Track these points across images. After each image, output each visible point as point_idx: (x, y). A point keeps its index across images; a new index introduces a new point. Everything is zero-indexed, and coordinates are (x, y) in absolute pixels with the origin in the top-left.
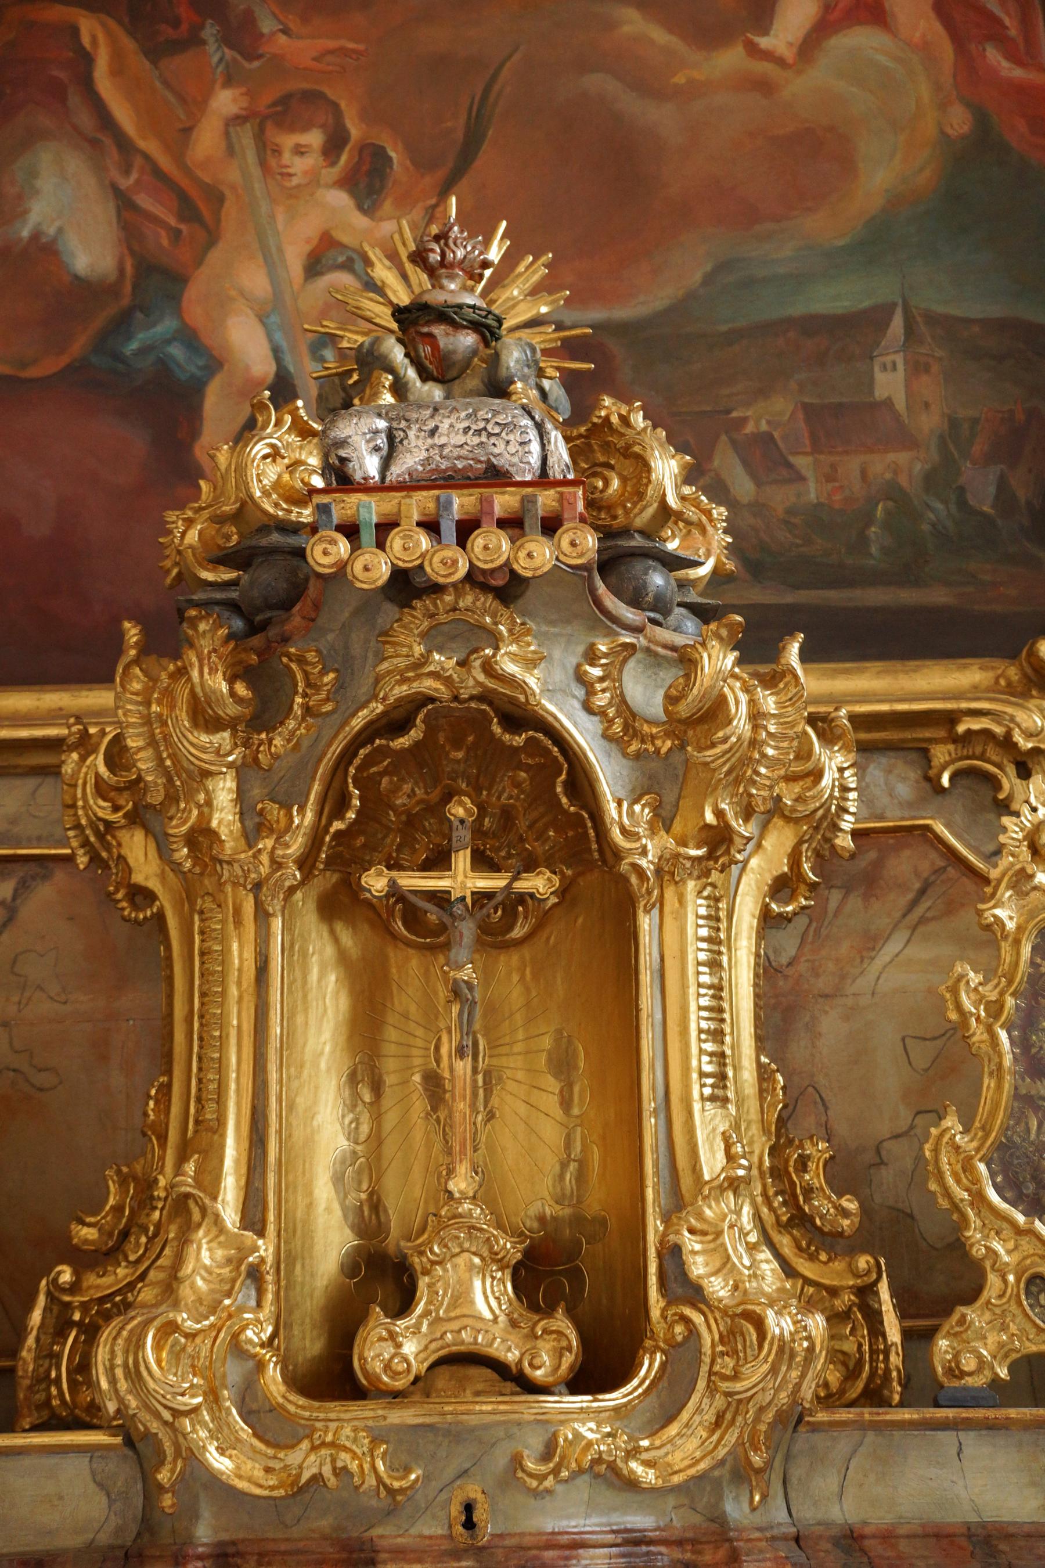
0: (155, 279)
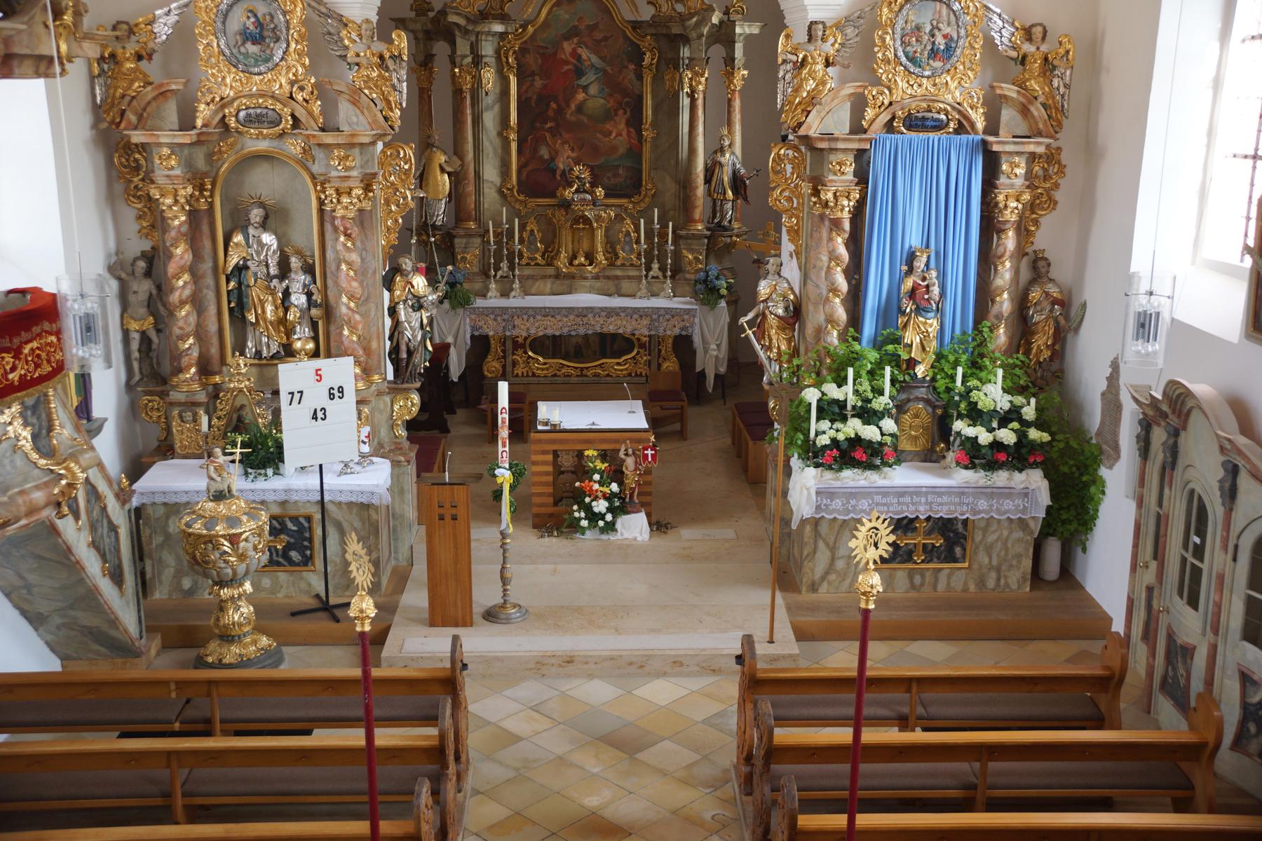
0: (552, 159)
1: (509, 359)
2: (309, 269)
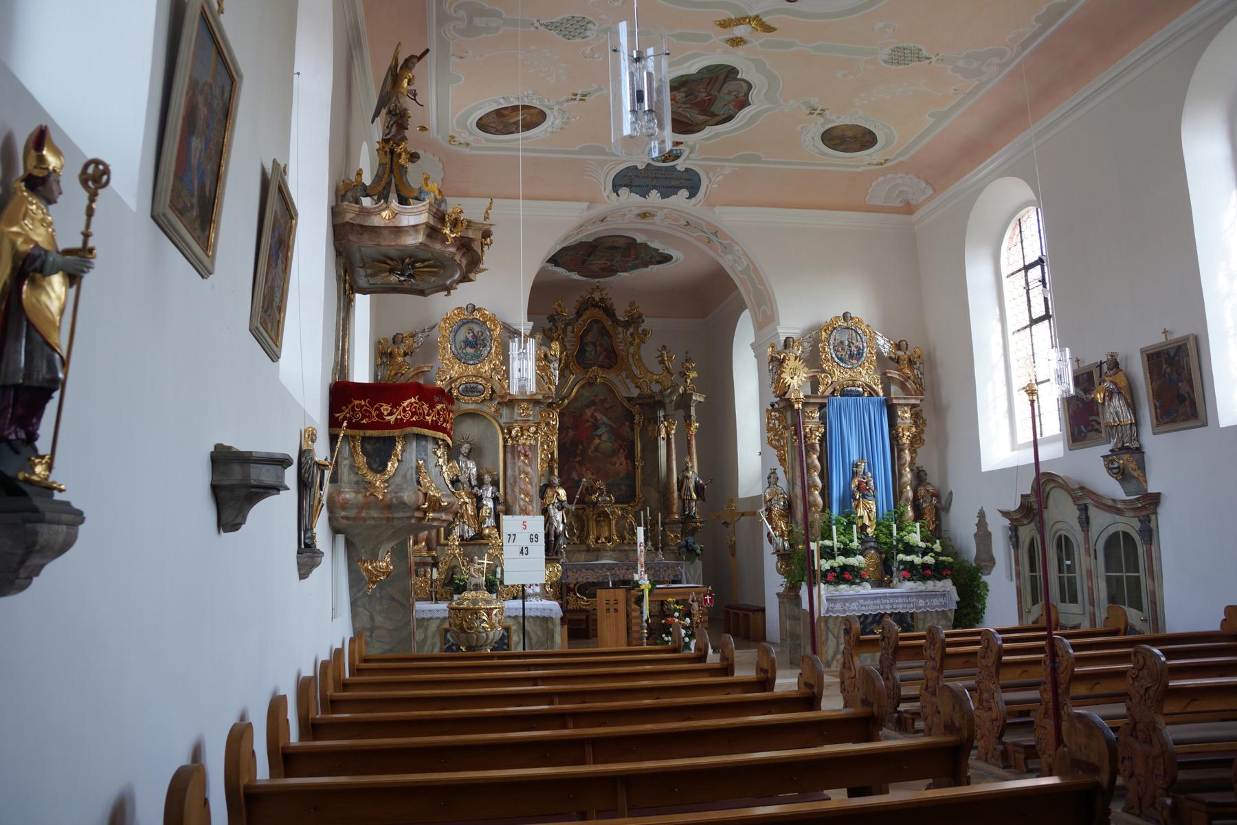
1: (565, 598)
2: (495, 483)
